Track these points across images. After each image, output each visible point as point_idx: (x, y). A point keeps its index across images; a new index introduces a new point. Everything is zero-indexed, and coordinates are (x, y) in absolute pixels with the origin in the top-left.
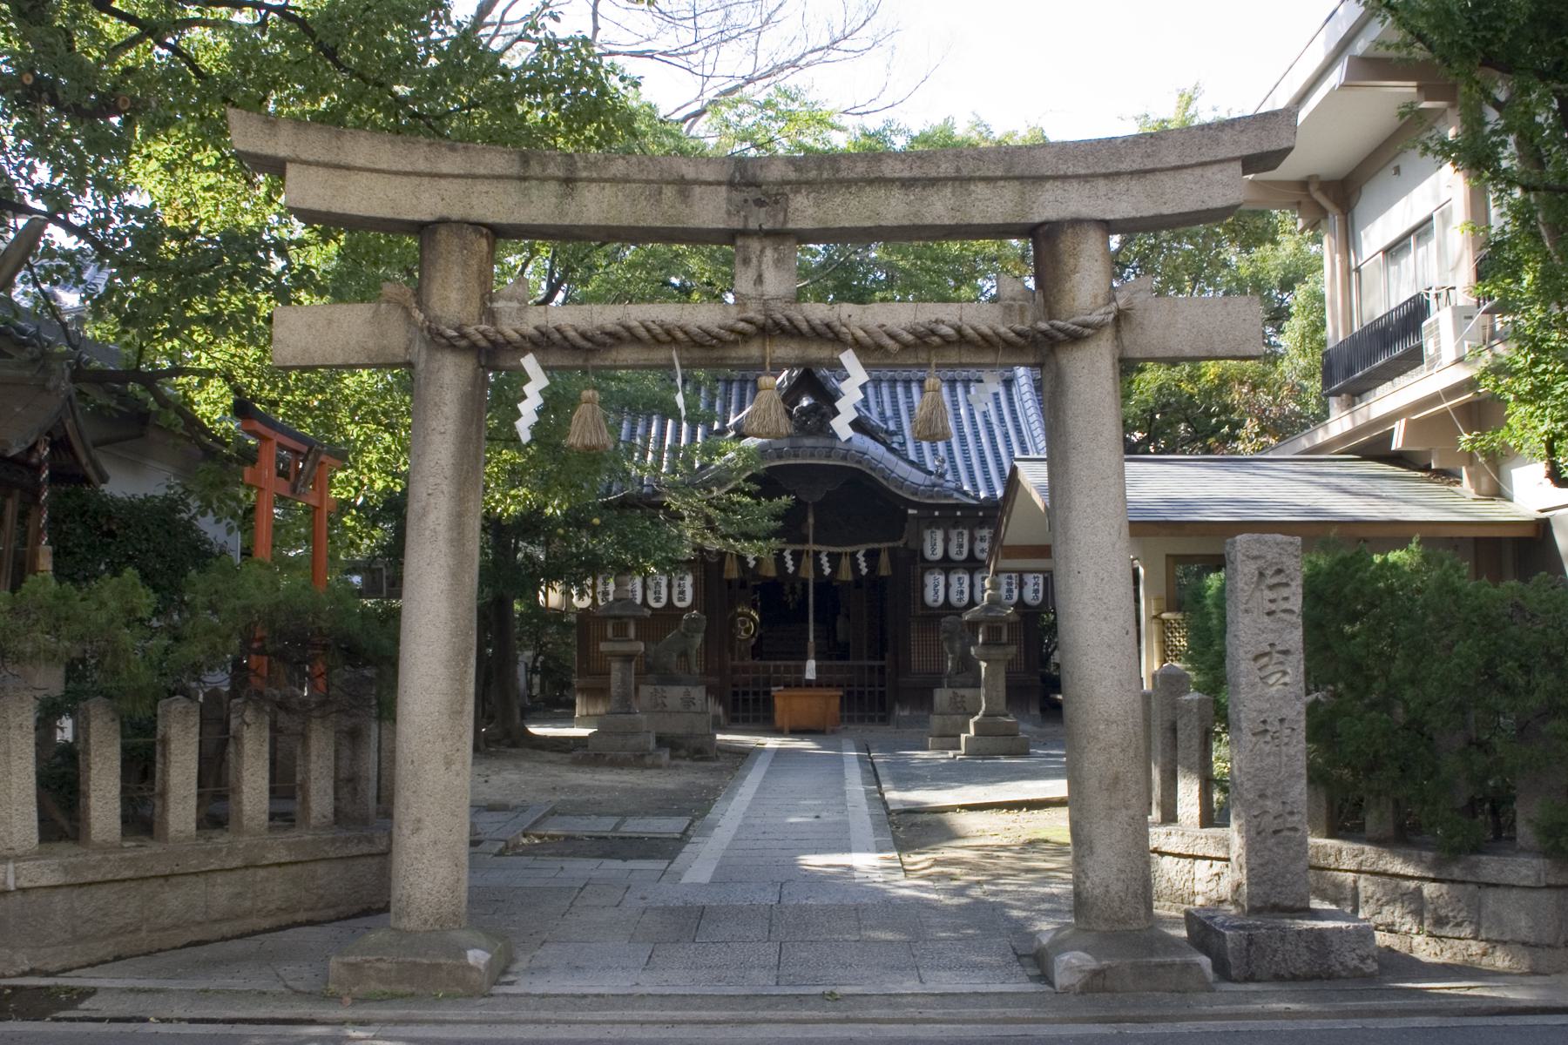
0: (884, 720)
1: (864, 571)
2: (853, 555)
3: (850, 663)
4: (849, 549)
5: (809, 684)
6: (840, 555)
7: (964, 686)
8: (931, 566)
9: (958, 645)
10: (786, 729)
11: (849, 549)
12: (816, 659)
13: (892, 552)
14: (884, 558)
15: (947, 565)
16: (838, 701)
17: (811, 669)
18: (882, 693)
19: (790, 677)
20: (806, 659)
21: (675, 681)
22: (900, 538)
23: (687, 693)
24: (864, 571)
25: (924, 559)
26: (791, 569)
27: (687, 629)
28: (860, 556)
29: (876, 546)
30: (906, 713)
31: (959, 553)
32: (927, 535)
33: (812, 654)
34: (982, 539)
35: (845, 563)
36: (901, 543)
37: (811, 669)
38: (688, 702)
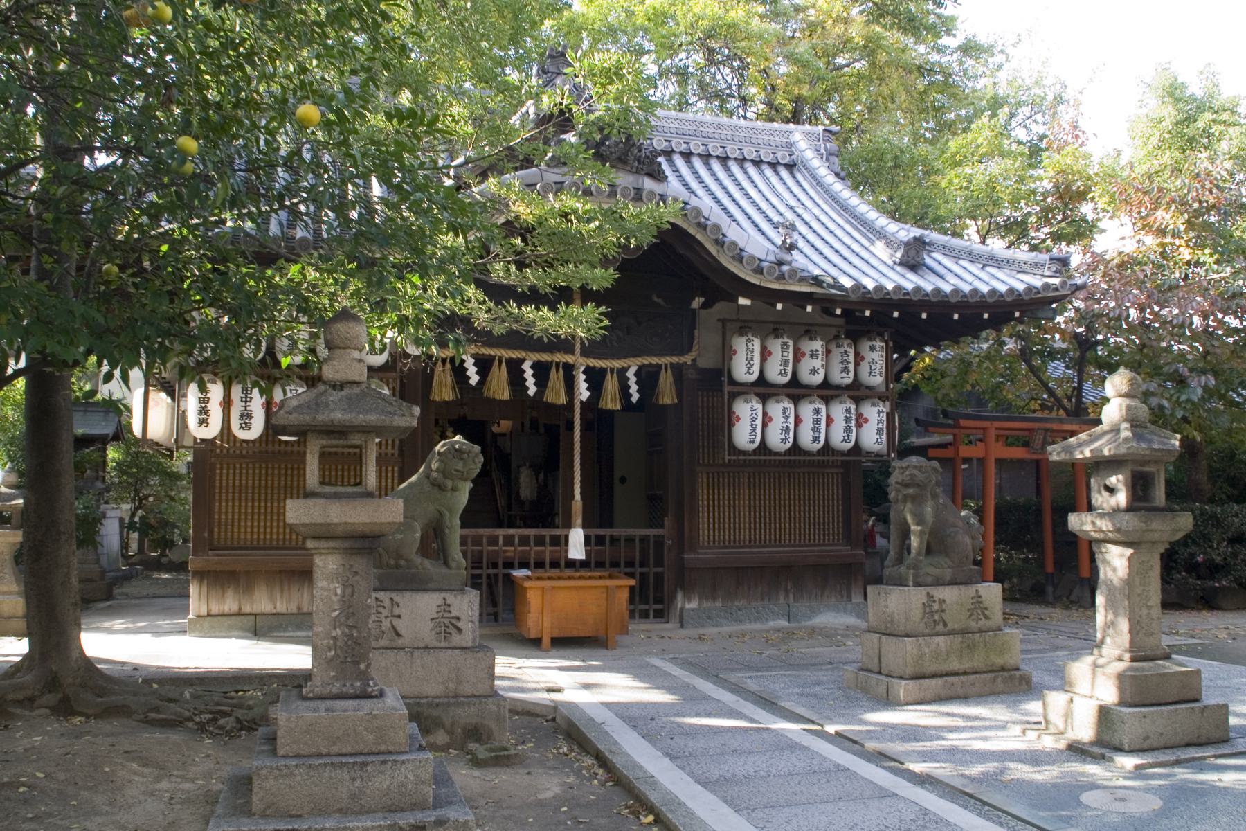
0: (660, 615)
1: (635, 397)
2: (622, 373)
3: (615, 532)
4: (617, 364)
5: (572, 564)
6: (602, 372)
7: (939, 582)
8: (741, 390)
9: (929, 510)
10: (546, 641)
11: (617, 364)
12: (584, 527)
13: (678, 370)
14: (666, 382)
15: (763, 389)
16: (625, 595)
17: (576, 548)
18: (659, 578)
19: (548, 552)
20: (569, 525)
21: (418, 584)
22: (690, 350)
23: (446, 605)
24: (635, 397)
25: (732, 381)
26: (532, 390)
27: (443, 472)
28: (630, 374)
29: (654, 360)
30: (692, 605)
31: (777, 374)
32: (740, 344)
33: (579, 521)
34: (813, 355)
35: (611, 385)
36: (687, 359)
37: (576, 548)
38: (447, 626)
